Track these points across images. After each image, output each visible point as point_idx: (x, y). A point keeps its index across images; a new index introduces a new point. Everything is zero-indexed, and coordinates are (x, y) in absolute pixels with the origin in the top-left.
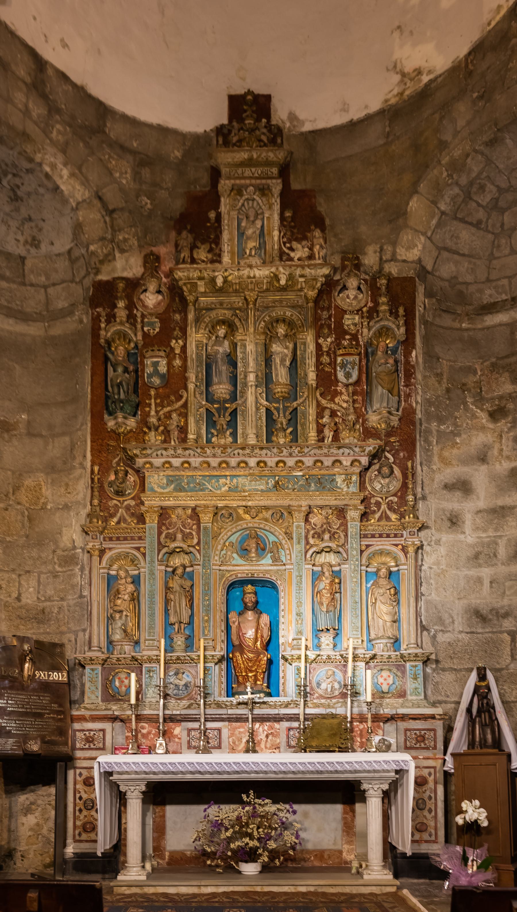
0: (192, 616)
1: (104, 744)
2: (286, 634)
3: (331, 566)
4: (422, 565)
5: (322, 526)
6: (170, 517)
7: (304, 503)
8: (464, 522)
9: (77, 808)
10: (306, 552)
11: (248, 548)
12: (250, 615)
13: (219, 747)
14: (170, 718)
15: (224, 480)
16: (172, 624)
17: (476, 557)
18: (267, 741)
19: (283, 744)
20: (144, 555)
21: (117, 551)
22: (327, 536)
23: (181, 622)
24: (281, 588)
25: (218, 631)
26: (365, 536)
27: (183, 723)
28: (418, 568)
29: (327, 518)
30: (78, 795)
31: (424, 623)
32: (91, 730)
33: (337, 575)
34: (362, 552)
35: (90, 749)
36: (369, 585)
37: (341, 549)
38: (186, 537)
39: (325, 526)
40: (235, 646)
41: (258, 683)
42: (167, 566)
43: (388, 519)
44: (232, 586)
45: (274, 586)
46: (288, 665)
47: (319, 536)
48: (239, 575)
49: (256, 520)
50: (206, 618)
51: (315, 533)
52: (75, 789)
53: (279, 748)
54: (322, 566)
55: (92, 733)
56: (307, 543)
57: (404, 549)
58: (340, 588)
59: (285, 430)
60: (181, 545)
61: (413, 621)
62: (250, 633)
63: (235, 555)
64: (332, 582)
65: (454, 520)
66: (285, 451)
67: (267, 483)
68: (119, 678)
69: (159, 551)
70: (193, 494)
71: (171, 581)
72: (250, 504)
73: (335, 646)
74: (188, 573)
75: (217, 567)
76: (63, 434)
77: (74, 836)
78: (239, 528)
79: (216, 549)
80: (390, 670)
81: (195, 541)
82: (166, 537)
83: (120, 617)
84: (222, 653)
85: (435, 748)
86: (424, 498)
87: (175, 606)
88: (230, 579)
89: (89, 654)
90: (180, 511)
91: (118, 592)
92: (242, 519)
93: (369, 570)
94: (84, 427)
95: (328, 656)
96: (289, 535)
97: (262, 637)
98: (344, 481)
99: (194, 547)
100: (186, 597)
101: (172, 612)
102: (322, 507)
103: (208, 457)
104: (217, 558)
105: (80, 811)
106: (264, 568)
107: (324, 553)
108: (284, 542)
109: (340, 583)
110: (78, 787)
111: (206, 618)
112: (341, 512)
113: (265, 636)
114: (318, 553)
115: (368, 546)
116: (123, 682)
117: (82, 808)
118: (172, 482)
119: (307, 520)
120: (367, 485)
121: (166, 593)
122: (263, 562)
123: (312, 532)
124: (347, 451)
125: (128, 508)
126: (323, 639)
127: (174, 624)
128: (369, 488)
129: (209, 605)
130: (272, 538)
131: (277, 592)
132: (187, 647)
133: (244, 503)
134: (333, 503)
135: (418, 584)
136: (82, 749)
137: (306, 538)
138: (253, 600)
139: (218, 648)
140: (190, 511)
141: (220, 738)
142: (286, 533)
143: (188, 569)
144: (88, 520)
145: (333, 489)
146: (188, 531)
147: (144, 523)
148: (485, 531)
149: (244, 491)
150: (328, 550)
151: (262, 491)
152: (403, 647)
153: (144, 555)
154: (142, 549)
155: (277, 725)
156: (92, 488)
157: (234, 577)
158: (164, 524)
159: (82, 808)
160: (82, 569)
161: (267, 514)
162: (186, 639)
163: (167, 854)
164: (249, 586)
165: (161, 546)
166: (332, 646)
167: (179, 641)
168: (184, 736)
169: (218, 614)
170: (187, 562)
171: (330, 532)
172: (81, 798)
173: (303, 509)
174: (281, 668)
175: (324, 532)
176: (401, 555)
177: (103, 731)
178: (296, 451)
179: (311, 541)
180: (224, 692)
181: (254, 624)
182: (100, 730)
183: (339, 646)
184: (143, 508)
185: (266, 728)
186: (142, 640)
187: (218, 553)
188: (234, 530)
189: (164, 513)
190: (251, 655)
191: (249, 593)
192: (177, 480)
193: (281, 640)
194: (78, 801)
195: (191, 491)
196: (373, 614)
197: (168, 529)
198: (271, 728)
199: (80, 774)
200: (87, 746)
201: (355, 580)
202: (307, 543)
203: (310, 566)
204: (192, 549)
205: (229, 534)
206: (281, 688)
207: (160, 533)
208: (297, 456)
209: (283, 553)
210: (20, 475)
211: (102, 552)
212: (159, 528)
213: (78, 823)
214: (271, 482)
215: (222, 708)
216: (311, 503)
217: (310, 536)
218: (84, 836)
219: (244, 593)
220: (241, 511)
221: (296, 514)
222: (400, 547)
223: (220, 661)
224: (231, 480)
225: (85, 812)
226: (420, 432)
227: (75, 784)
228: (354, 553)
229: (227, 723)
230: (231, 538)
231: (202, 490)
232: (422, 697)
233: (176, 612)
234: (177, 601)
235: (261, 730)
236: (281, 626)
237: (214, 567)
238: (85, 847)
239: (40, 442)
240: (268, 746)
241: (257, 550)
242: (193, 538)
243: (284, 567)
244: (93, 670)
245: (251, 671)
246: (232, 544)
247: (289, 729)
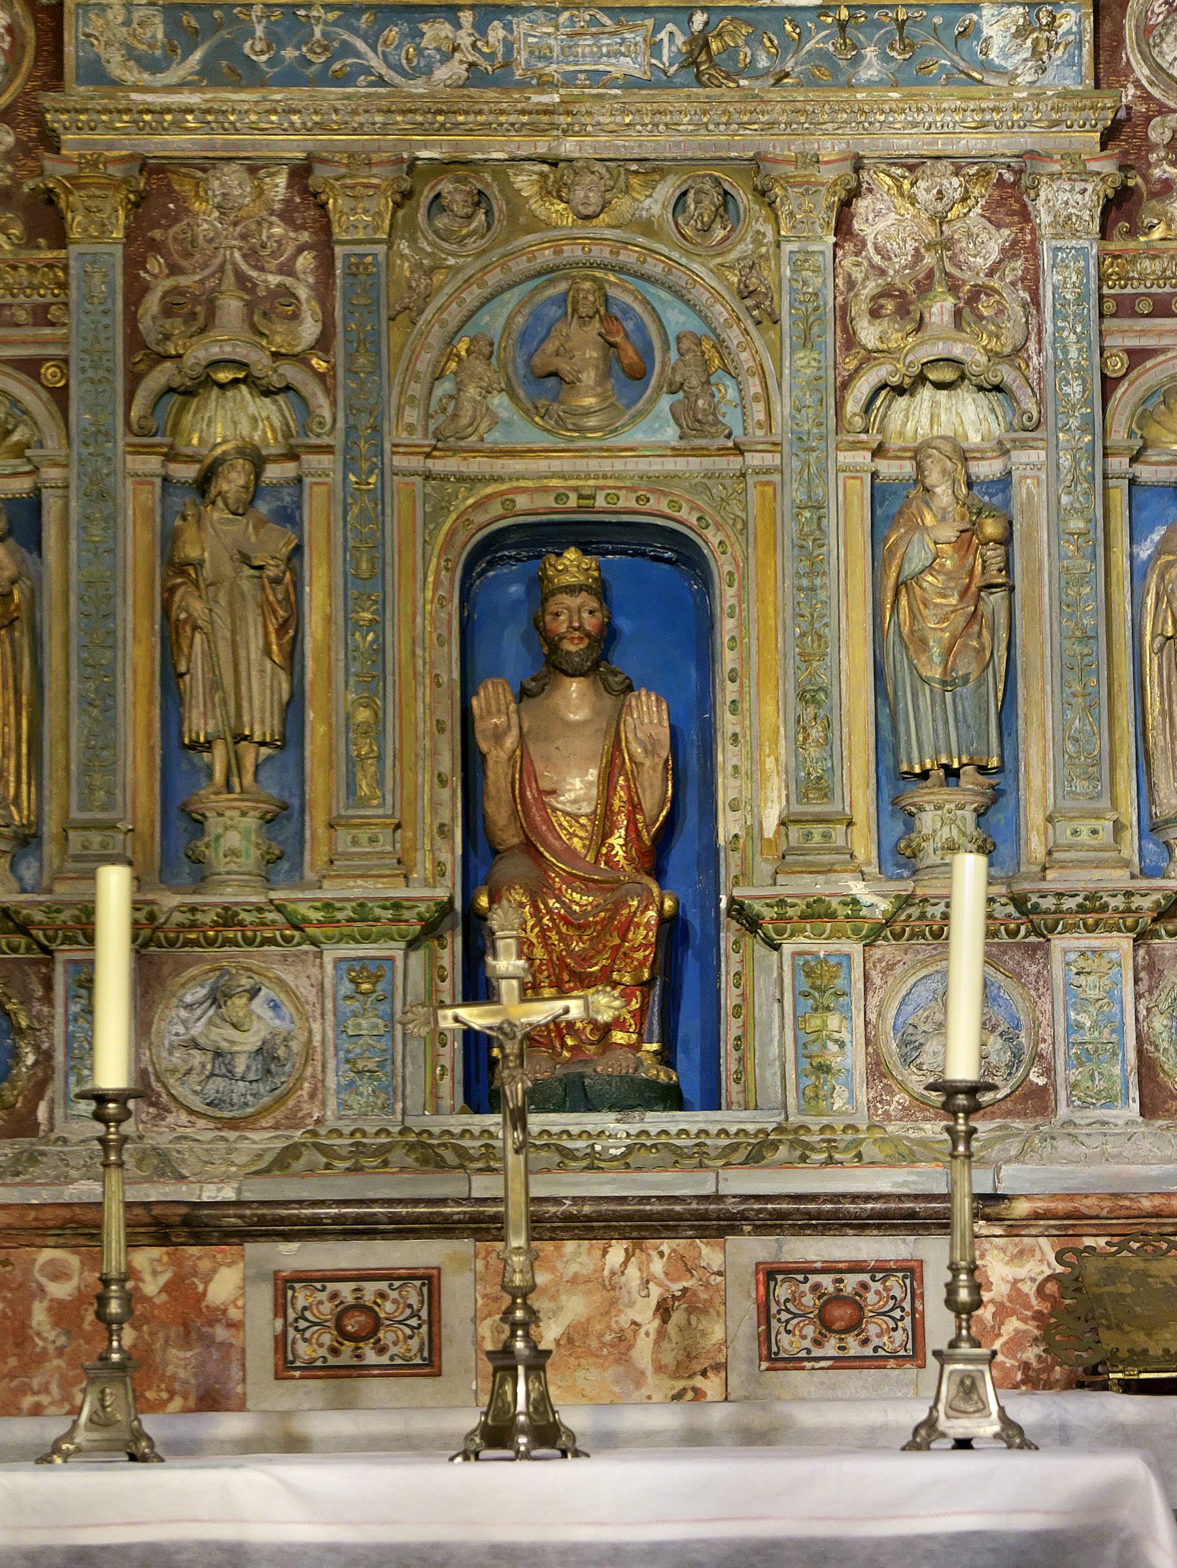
0: (293, 708)
2: (754, 798)
3: (965, 456)
5: (918, 256)
6: (184, 211)
7: (830, 147)
10: (845, 386)
11: (564, 367)
12: (575, 698)
14: (186, 1222)
16: (194, 746)
18: (661, 1334)
20: (60, 396)
22: (940, 308)
23: (240, 738)
24: (722, 566)
25: (425, 779)
26: (1126, 307)
27: (252, 1249)
29: (940, 219)
33: (990, 498)
34: (1108, 384)
36: (1144, 553)
37: (1006, 374)
38: (271, 308)
39: (929, 259)
42: (171, 456)
44: (489, 551)
45: (684, 555)
46: (761, 950)
47: (903, 304)
48: (522, 502)
49: (601, 227)
50: (363, 715)
51: (886, 293)
54: (917, 455)
58: (1007, 567)
60: (241, 352)
62: (577, 789)
63: (499, 402)
64: (968, 538)
67: (655, 48)
69: (134, 380)
70: (297, 95)
71: (190, 532)
72: (569, 147)
74: (276, 488)
75: (416, 463)
78: (520, 265)
79: (411, 373)
81: (309, 330)
82: (168, 311)
84: (442, 893)
87: (211, 655)
88: (480, 518)
90: (232, 179)
92: (536, 225)
93: (1145, 473)
96: (756, 302)
97: (634, 807)
98: (1021, 33)
99: (301, 359)
100: (266, 608)
101: (196, 684)
102: (913, 165)
104: (412, 415)
106: (643, 465)
107: (926, 393)
108: (734, 336)
109: (1006, 541)
111: (363, 715)
112: (1011, 193)
113: (649, 801)
114: (900, 391)
115: (1137, 356)
118: (193, 38)
119: (843, 227)
120: (1131, 53)
121: (170, 591)
122: (636, 436)
123: (871, 287)
126: (928, 821)
127: (208, 746)
128: (1142, 71)
129: (379, 650)
130: (677, 319)
131: (706, 581)
132: (271, 861)
133: (542, 146)
134: (972, 143)
137: (843, 314)
138: (591, 623)
139: (423, 866)
140: (282, 180)
141: (434, 1320)
142: (744, 293)
143: (273, 472)
145: (972, 75)
146: (274, 280)
147: (60, 240)
149: (545, 84)
150: (948, 375)
151: (631, 83)
153: (60, 396)
154: (49, 371)
155: (710, 1254)
157: (496, 509)
158: (155, 247)
161: (655, 202)
162: (269, 821)
164: (571, 555)
165: (142, 354)
169: (426, 693)
170: (267, 437)
171: (954, 288)
173: (828, 175)
174: (730, 964)
175: (924, 286)
179: (868, 334)
180: (451, 1089)
181: (600, 746)
184: (55, 169)
185: (657, 1266)
186: (51, 827)
188: (494, 278)
189: (155, 191)
190: (580, 900)
191: (571, 590)
192: (218, 26)
193: (728, 826)
195: (291, 77)
197: (174, 270)
198: (683, 1265)
201: (1077, 524)
202: (850, 341)
204: (291, 373)
205: (473, 294)
206: (729, 1062)
207: (135, 292)
209: (732, 393)
212: (133, 263)
214: (673, 41)
215: (441, 1165)
216: (868, 146)
217: (859, 308)
219: (541, 590)
220: (525, 182)
221: (789, 201)
223: (431, 930)
224: (481, 28)
228: (1075, 389)
229: (465, 1246)
230: (484, 318)
231: (344, 79)
233: (215, 685)
234: (224, 632)
236: (726, 756)
237: (400, 462)
241: (605, 374)
242: (295, 316)
243: (735, 463)
246: (486, 351)
247: (770, 1273)
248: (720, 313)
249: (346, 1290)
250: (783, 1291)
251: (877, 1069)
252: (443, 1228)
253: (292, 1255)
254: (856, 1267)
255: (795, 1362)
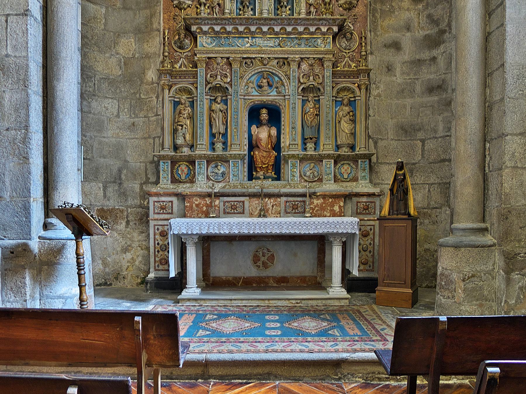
0: (226, 129)
1: (172, 210)
2: (285, 141)
4: (370, 97)
8: (395, 69)
9: (156, 250)
10: (298, 87)
13: (243, 213)
15: (247, 39)
17: (403, 91)
19: (283, 211)
21: (179, 86)
28: (367, 99)
30: (156, 242)
31: (370, 134)
32: (164, 202)
34: (333, 87)
35: (163, 213)
36: (337, 109)
37: (320, 87)
40: (253, 146)
41: (269, 171)
43: (350, 66)
48: (256, 102)
49: (267, 66)
51: (304, 75)
52: (155, 238)
53: (280, 213)
55: (165, 203)
56: (299, 81)
57: (359, 87)
59: (286, 7)
61: (363, 134)
65: (390, 68)
66: (286, 21)
68: (181, 169)
72: (263, 56)
73: (315, 149)
74: (224, 100)
75: (243, 97)
76: (146, 8)
77: (155, 267)
80: (349, 164)
81: (229, 80)
82: (211, 77)
83: (182, 129)
84: (245, 153)
85: (374, 213)
86: (371, 53)
89: (162, 153)
91: (180, 113)
93: (338, 99)
94: (159, 4)
95: (311, 155)
103: (237, 25)
104: (242, 91)
105: (158, 251)
110: (156, 237)
116: (183, 171)
117: (160, 250)
123: (302, 74)
124: (325, 22)
125: (186, 57)
132: (223, 149)
135: (367, 109)
136: (159, 213)
144: (161, 66)
148: (408, 75)
152: (357, 149)
153: (197, 88)
155: (279, 200)
156: (164, 44)
157: (253, 103)
159: (160, 250)
160: (157, 97)
163: (211, 279)
165: (207, 83)
166: (313, 149)
167: (219, 146)
168: (222, 204)
172: (158, 244)
176: (357, 90)
177: (172, 202)
178: (293, 22)
179: (302, 81)
182: (170, 202)
183: (318, 148)
185: (272, 201)
187: (242, 87)
193: (282, 145)
194: (156, 245)
196: (339, 128)
197: (212, 71)
199: (158, 229)
200: (162, 212)
202: (299, 81)
203: (301, 97)
205: (250, 75)
207: (206, 74)
208: (293, 25)
210: (119, 35)
211: (170, 87)
213: (157, 259)
218: (161, 267)
221: (292, 63)
222: (356, 85)
225: (161, 253)
226: (370, 10)
227: (155, 235)
229: (248, 198)
232: (368, 181)
233: (216, 126)
235: (269, 202)
237: (241, 97)
238: (161, 274)
239: (131, 13)
240: (273, 212)
244: (164, 163)
245: (265, 164)
248: (282, 78)
249: (233, 203)
250: (288, 204)
251: (301, 176)
252: (245, 196)
253: (226, 199)
254: (297, 201)
255: (289, 213)
